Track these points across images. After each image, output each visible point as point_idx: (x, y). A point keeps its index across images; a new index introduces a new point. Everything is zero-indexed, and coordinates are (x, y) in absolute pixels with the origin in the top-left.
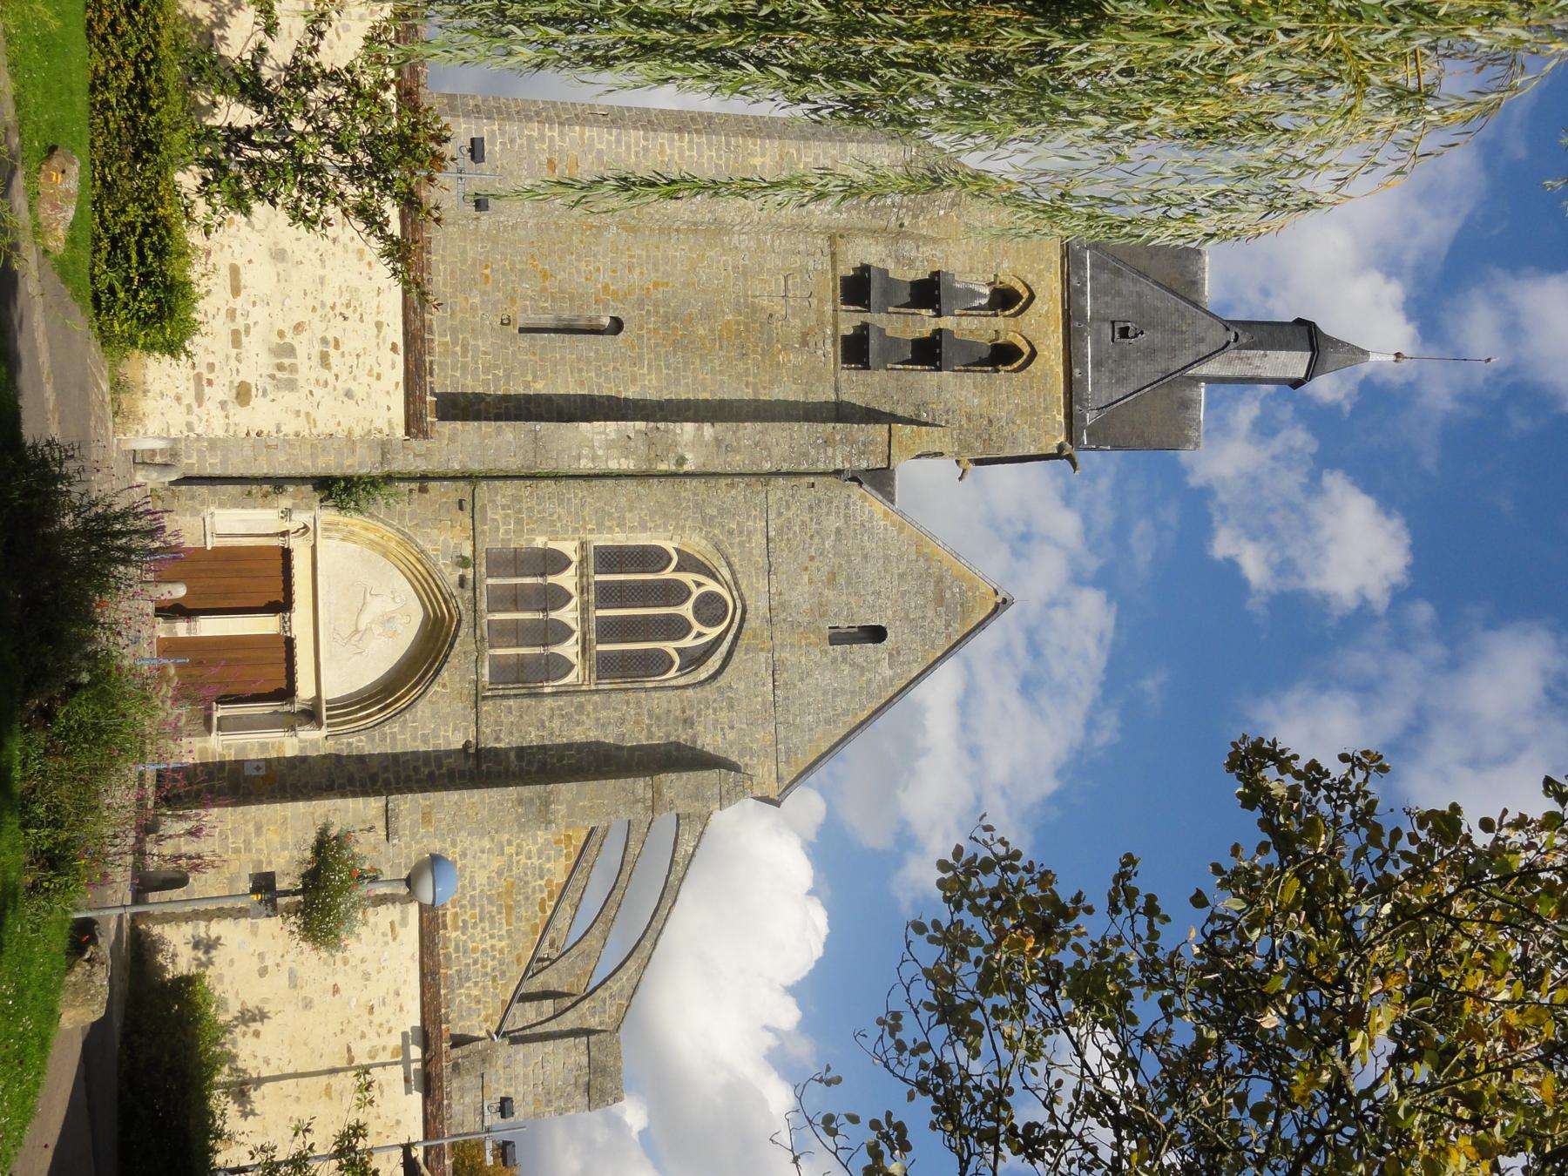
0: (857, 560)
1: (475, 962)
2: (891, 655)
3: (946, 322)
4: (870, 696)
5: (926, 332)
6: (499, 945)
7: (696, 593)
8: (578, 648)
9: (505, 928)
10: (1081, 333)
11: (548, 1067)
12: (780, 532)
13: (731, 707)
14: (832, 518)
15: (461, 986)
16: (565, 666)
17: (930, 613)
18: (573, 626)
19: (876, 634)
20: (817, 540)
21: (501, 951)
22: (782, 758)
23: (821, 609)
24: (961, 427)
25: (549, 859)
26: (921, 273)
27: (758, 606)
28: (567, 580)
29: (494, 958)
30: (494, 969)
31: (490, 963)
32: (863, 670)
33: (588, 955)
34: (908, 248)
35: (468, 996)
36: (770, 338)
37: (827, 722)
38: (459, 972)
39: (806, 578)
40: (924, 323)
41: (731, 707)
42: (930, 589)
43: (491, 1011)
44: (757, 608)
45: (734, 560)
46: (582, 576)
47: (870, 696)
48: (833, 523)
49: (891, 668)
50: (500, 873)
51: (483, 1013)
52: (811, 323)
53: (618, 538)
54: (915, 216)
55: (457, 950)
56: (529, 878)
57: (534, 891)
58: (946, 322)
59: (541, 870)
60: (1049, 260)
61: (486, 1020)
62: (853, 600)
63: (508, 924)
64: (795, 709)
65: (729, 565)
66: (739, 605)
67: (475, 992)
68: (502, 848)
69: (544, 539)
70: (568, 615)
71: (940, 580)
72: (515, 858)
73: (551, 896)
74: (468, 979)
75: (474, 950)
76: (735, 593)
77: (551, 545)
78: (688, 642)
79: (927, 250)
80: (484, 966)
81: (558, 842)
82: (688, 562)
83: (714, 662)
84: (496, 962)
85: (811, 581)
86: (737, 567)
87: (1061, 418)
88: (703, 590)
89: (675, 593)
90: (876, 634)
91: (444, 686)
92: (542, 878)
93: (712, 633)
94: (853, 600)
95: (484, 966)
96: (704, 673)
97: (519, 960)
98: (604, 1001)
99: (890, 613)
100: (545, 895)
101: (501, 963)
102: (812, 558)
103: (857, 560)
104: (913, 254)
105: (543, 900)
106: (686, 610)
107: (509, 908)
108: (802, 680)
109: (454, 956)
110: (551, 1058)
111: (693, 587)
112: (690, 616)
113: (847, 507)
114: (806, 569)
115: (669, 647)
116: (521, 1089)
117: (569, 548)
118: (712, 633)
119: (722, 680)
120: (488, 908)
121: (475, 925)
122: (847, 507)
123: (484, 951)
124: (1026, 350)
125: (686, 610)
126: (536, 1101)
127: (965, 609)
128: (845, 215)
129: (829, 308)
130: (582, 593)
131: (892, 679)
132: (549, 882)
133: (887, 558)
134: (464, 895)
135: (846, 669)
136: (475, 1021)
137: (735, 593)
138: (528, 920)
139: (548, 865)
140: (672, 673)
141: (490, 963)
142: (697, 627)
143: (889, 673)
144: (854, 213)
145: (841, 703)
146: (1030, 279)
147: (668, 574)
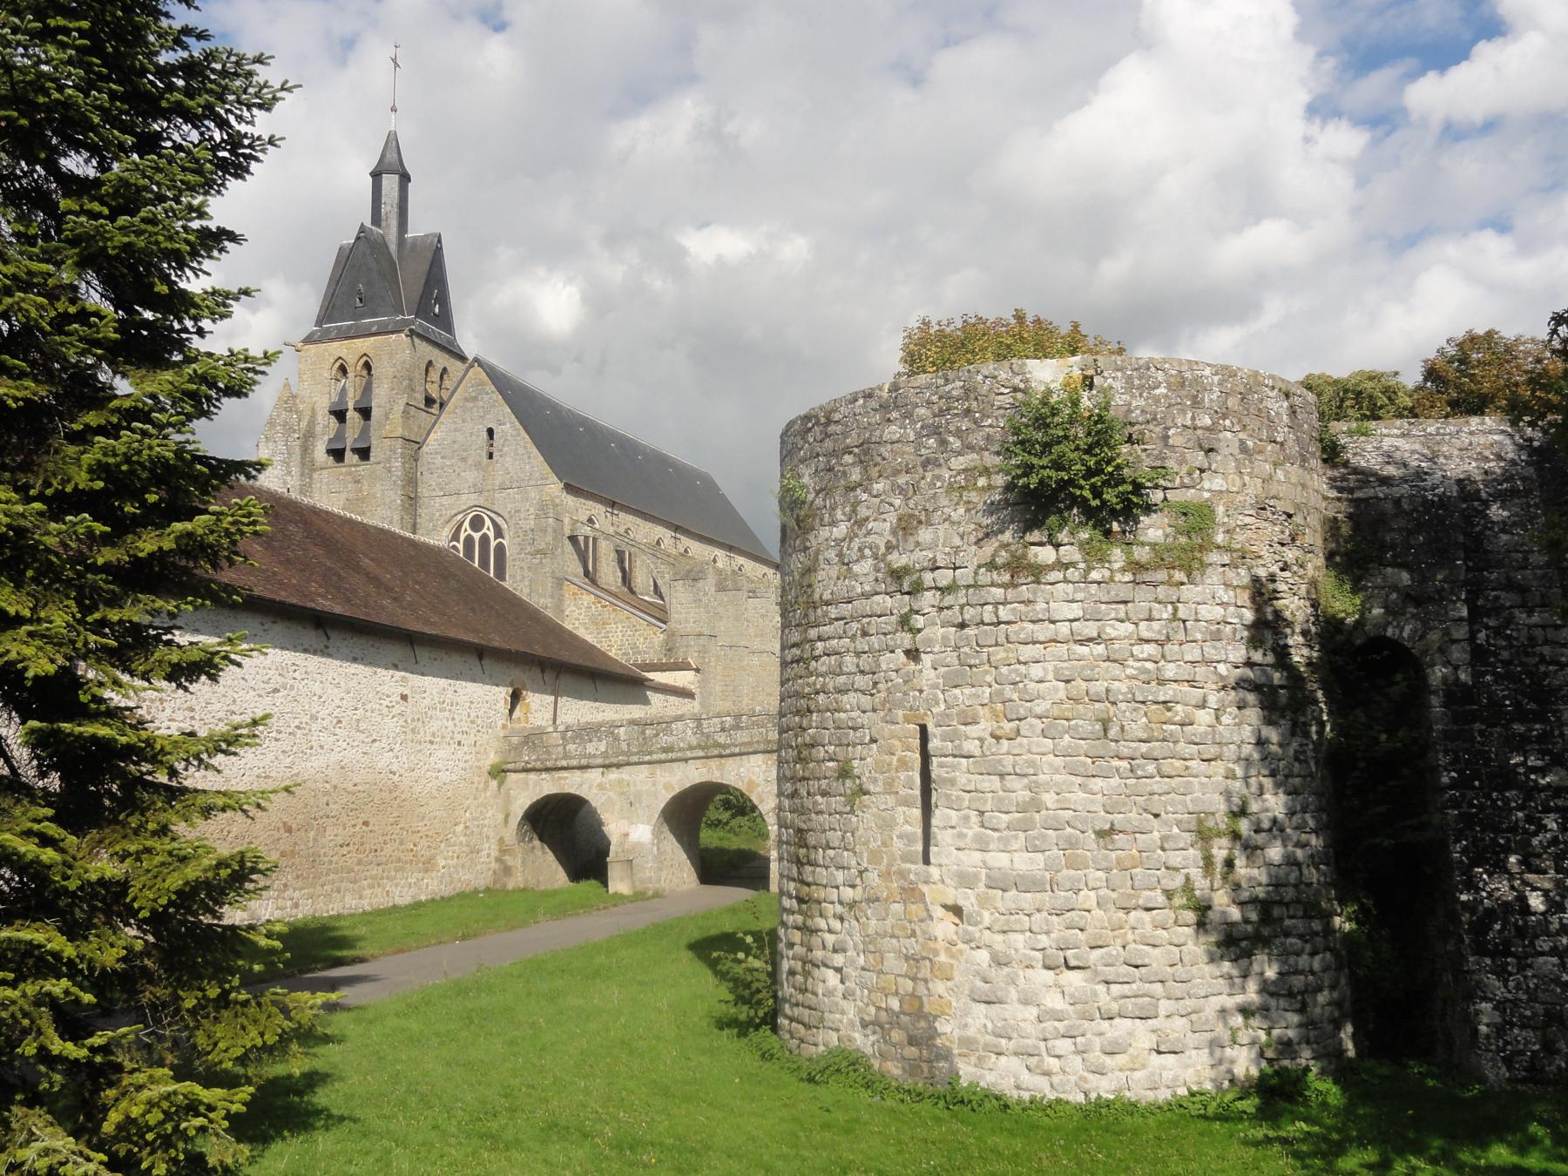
0: (456, 446)
3: (351, 405)
4: (519, 435)
5: (357, 415)
7: (469, 531)
10: (357, 327)
12: (442, 489)
13: (518, 511)
17: (481, 404)
19: (490, 432)
22: (544, 482)
23: (478, 465)
26: (333, 419)
27: (473, 499)
34: (319, 429)
36: (357, 500)
37: (529, 458)
40: (351, 415)
41: (518, 511)
42: (470, 405)
45: (453, 512)
47: (519, 435)
48: (438, 461)
50: (587, 629)
52: (349, 478)
54: (294, 431)
58: (351, 405)
60: (325, 350)
62: (474, 447)
64: (522, 475)
67: (642, 640)
71: (466, 399)
79: (319, 419)
83: (499, 520)
87: (394, 336)
89: (469, 540)
90: (490, 432)
93: (488, 522)
94: (474, 447)
96: (504, 526)
103: (456, 446)
112: (480, 534)
115: (493, 544)
118: (488, 522)
119: (507, 517)
124: (365, 358)
125: (477, 536)
126: (699, 607)
127: (482, 384)
129: (344, 470)
133: (455, 430)
136: (656, 640)
142: (485, 530)
145: (521, 450)
146: (332, 361)
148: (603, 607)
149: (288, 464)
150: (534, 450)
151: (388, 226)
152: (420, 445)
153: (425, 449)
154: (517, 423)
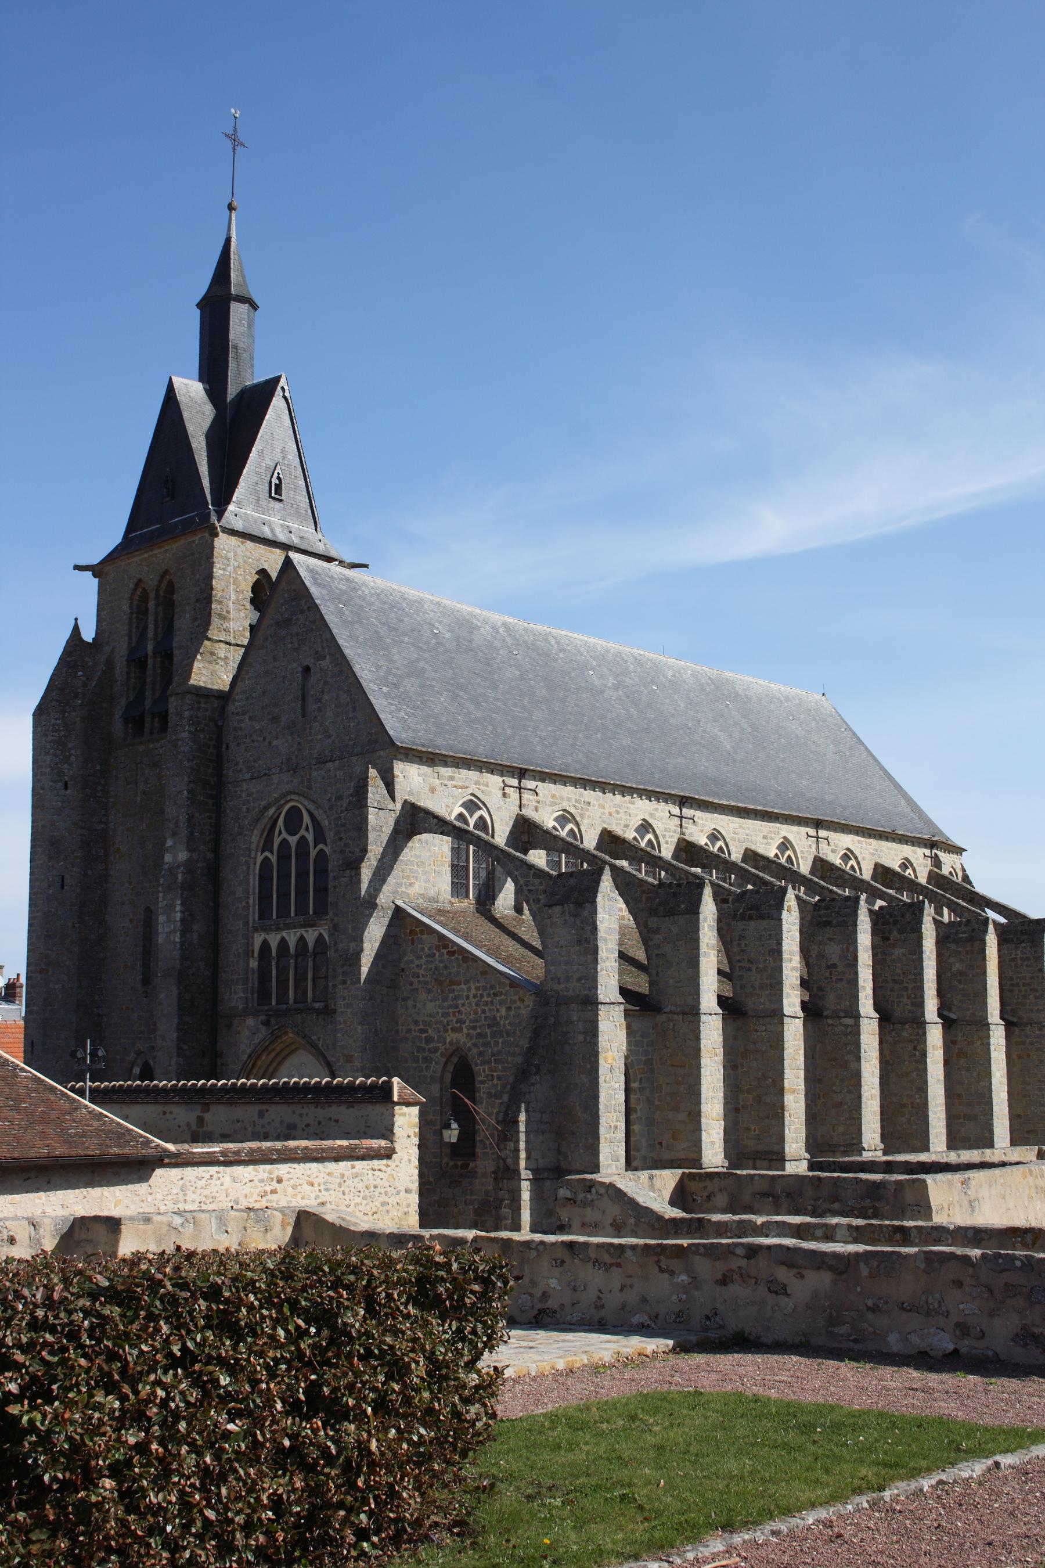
1: (484, 1012)
2: (318, 659)
6: (473, 991)
7: (284, 835)
8: (310, 930)
9: (463, 986)
14: (243, 725)
15: (498, 1024)
16: (320, 938)
17: (295, 629)
18: (298, 934)
20: (255, 737)
21: (478, 989)
24: (199, 626)
25: (423, 949)
28: (274, 940)
29: (482, 996)
30: (489, 995)
32: (326, 683)
33: (628, 884)
35: (506, 1017)
37: (354, 709)
38: (490, 1026)
39: (275, 743)
43: (517, 997)
44: (288, 783)
46: (271, 930)
49: (324, 658)
50: (429, 991)
53: (253, 900)
54: (76, 696)
55: (474, 1028)
57: (442, 961)
59: (428, 956)
63: (459, 984)
65: (266, 808)
67: (503, 1011)
68: (414, 990)
69: (251, 960)
70: (292, 938)
71: (278, 624)
72: (421, 979)
74: (494, 1018)
75: (476, 1013)
76: (282, 802)
77: (256, 954)
78: (310, 838)
80: (487, 1005)
81: (413, 941)
82: (267, 845)
84: (485, 994)
85: (277, 738)
88: (283, 829)
91: (319, 1039)
92: (435, 955)
93: (306, 819)
95: (487, 1004)
96: (325, 823)
99: (295, 665)
100: (445, 951)
101: (485, 988)
102: (264, 739)
105: (449, 953)
106: (293, 840)
107: (452, 983)
108: (330, 737)
109: (479, 1031)
110: (557, 939)
111: (282, 837)
113: (238, 714)
114: (270, 743)
115: (313, 853)
116: (575, 968)
117: (258, 939)
118: (306, 819)
121: (460, 1012)
122: (238, 714)
123: (477, 1005)
128: (73, 752)
132: (438, 948)
134: (441, 1022)
135: (326, 697)
137: (282, 802)
138: (459, 966)
140: (326, 849)
141: (485, 999)
142: (303, 832)
144: (70, 745)
147: (274, 859)
153: (231, 708)
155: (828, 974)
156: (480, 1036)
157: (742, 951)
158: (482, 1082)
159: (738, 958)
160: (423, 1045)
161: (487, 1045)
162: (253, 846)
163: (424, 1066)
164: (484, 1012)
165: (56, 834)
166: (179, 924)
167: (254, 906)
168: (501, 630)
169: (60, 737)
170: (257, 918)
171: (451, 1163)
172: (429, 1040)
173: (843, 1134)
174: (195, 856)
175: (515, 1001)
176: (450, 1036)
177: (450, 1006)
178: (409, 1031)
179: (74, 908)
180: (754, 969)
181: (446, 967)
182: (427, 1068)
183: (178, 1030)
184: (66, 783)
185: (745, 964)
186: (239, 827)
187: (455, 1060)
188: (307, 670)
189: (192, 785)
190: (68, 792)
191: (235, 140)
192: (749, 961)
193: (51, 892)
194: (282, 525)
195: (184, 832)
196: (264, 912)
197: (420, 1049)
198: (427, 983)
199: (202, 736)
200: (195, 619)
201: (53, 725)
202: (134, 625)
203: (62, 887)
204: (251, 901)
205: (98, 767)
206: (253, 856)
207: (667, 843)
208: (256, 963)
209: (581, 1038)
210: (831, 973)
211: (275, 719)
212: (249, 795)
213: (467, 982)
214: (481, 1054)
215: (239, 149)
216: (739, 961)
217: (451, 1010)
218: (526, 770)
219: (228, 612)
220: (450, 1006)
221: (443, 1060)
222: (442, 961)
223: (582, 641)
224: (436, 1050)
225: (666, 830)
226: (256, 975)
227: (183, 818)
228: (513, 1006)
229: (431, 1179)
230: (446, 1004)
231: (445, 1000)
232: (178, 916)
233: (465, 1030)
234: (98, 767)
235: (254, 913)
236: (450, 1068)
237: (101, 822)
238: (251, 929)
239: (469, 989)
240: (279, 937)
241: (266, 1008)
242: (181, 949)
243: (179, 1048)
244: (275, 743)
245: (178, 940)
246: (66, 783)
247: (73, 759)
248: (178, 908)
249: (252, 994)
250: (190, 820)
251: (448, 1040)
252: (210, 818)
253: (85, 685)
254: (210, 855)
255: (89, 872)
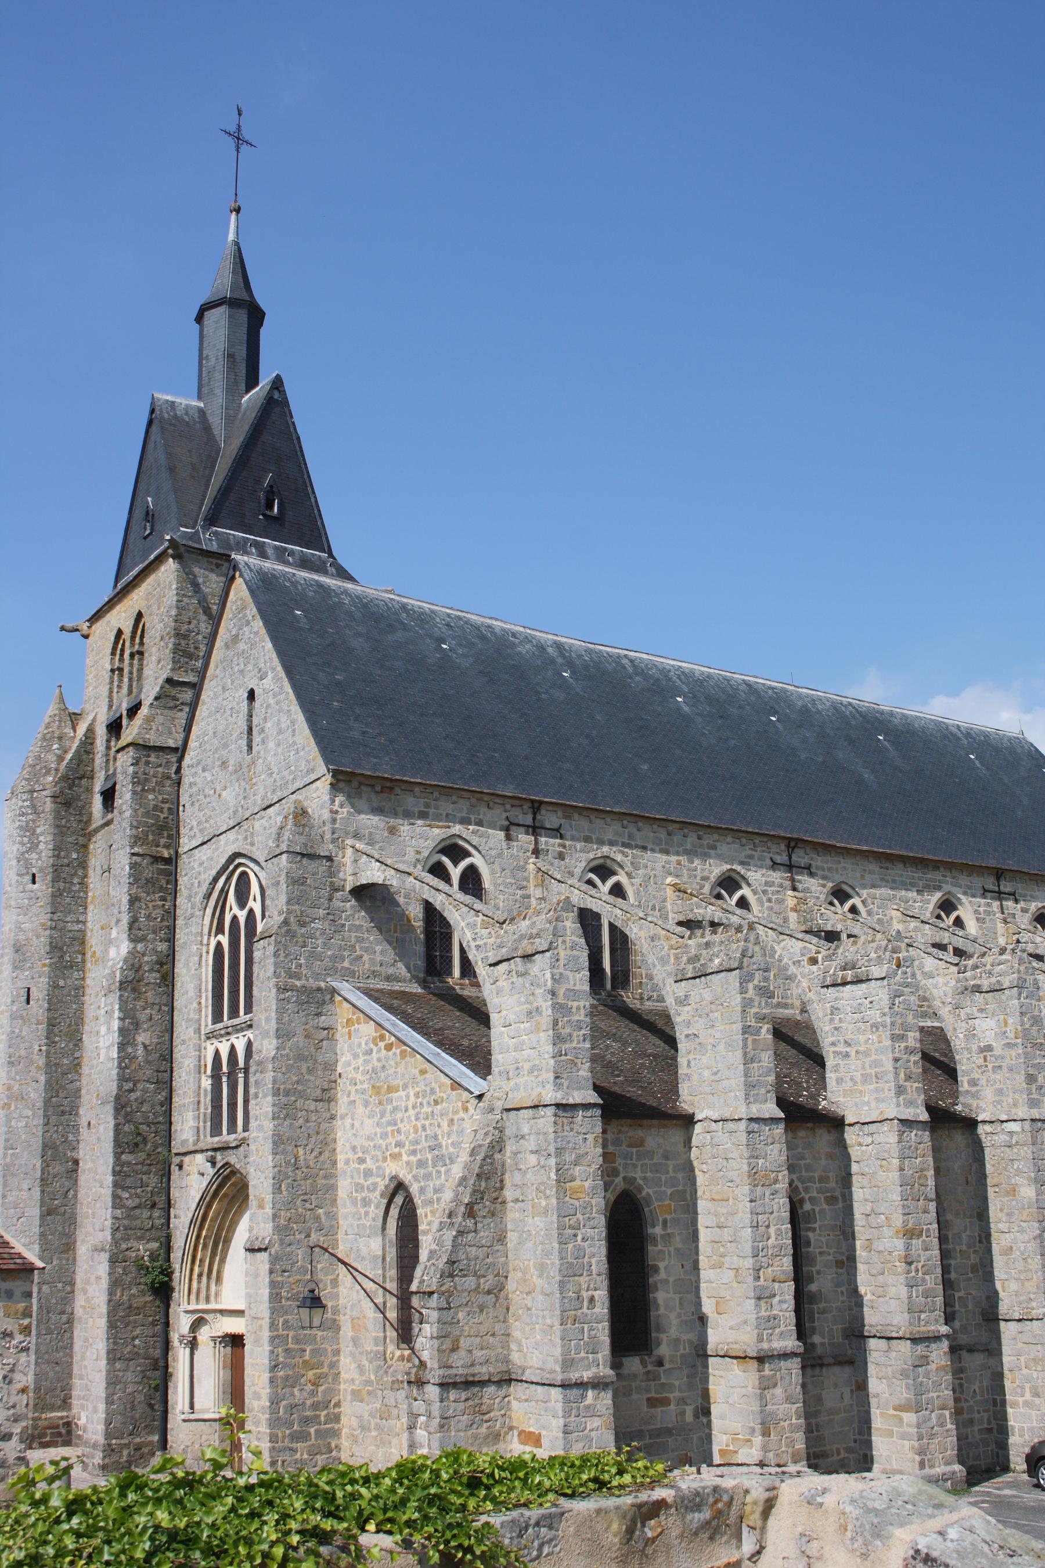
2: (261, 679)
4: (281, 688)
6: (412, 1099)
7: (236, 910)
11: (512, 1017)
15: (440, 1146)
21: (417, 1095)
25: (360, 1045)
31: (426, 1109)
42: (230, 653)
43: (460, 1104)
46: (222, 1036)
50: (366, 1104)
51: (462, 1114)
54: (48, 772)
55: (414, 1152)
56: (369, 1067)
61: (466, 1109)
62: (235, 735)
65: (215, 880)
66: (237, 862)
72: (358, 1087)
73: (382, 1038)
74: (436, 1137)
75: (416, 1132)
76: (231, 867)
80: (427, 1118)
86: (214, 872)
92: (372, 1050)
97: (423, 1072)
98: (478, 947)
100: (382, 1044)
104: (100, 755)
107: (391, 1089)
109: (419, 1156)
114: (219, 796)
120: (388, 1117)
121: (399, 1131)
122: (193, 766)
123: (417, 1119)
126: (537, 1029)
128: (41, 838)
130: (228, 1034)
131: (273, 669)
132: (375, 1042)
137: (231, 867)
139: (363, 1045)
142: (251, 903)
143: (270, 675)
144: (38, 830)
147: (224, 940)
148: (389, 1047)
149: (34, 833)
150: (300, 717)
151: (211, 392)
152: (180, 752)
153: (187, 761)
154: (280, 668)
155: (981, 1061)
156: (421, 1164)
157: (836, 1029)
158: (426, 1232)
159: (831, 1039)
160: (362, 1181)
161: (428, 1177)
162: (206, 930)
163: (362, 1211)
164: (424, 1128)
165: (21, 937)
166: (116, 1034)
167: (207, 1007)
168: (550, 650)
169: (27, 822)
170: (210, 1022)
171: (398, 1353)
172: (368, 1173)
173: (1017, 1294)
174: (140, 947)
175: (456, 1112)
176: (393, 1168)
177: (389, 1123)
178: (347, 1162)
179: (40, 1027)
180: (853, 1054)
181: (384, 1067)
182: (367, 1213)
183: (115, 1173)
184: (34, 876)
185: (841, 1048)
186: (192, 908)
187: (399, 1200)
188: (251, 695)
189: (138, 859)
190: (35, 886)
191: (239, 139)
192: (847, 1043)
193: (14, 1009)
194: (276, 548)
195: (125, 919)
196: (217, 1017)
197: (359, 1187)
198: (363, 1092)
199: (151, 797)
200: (159, 662)
201: (22, 807)
202: (116, 684)
203: (28, 1003)
204: (203, 1001)
205: (74, 856)
206: (205, 942)
207: (769, 900)
208: (210, 1082)
209: (533, 1159)
210: (985, 1060)
211: (224, 764)
212: (201, 864)
213: (405, 1087)
214: (422, 1190)
215: (244, 148)
216: (833, 1044)
217: (389, 1129)
218: (541, 803)
219: (196, 648)
220: (389, 1123)
221: (385, 1201)
222: (379, 1060)
223: (673, 666)
224: (375, 1185)
225: (767, 883)
226: (209, 1097)
227: (125, 899)
228: (456, 1117)
229: (373, 1377)
230: (384, 1120)
231: (382, 1115)
232: (116, 1024)
233: (405, 1158)
234: (74, 856)
235: (206, 1016)
236: (394, 1212)
237: (78, 922)
238: (203, 1037)
239: (408, 1097)
240: (229, 1043)
241: (216, 1139)
242: (120, 1067)
243: (115, 1196)
244: (224, 794)
245: (116, 1056)
246: (34, 876)
247: (42, 846)
248: (117, 1014)
249: (205, 1122)
250: (133, 901)
251: (387, 1172)
252: (164, 899)
253: (60, 759)
254: (163, 947)
255: (61, 983)
